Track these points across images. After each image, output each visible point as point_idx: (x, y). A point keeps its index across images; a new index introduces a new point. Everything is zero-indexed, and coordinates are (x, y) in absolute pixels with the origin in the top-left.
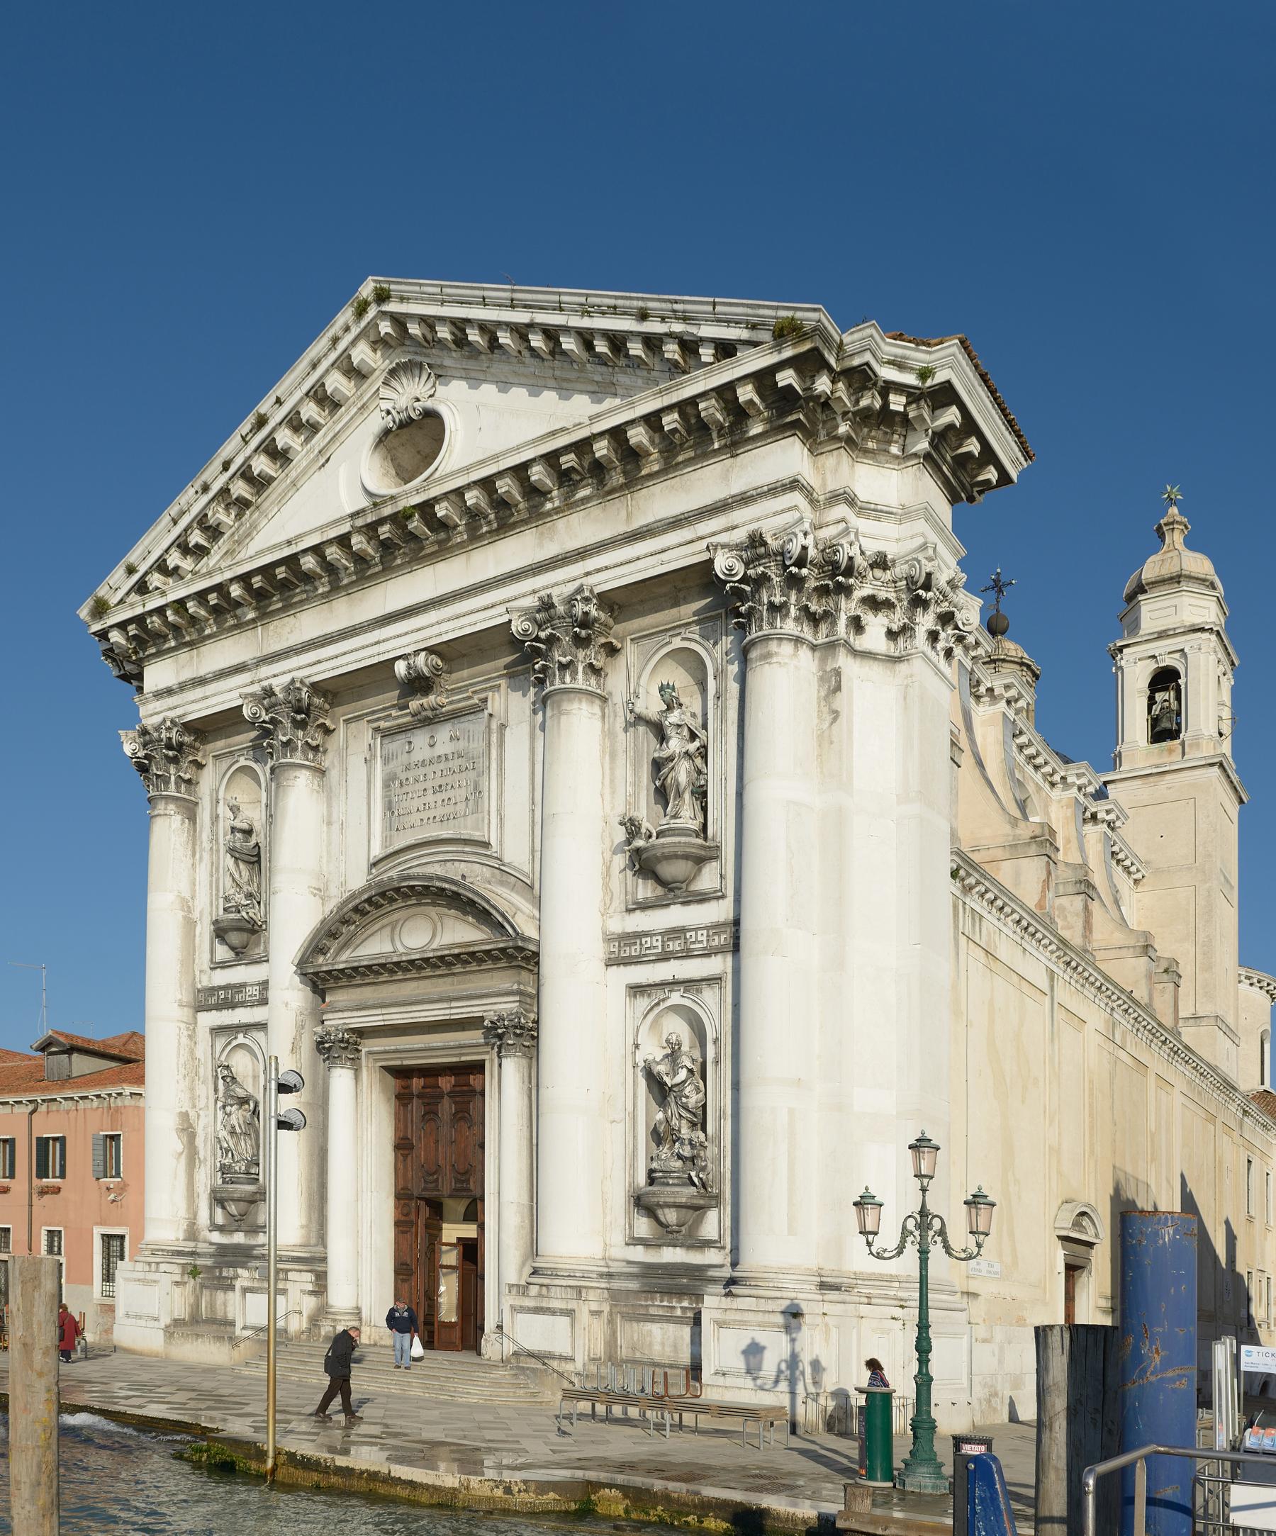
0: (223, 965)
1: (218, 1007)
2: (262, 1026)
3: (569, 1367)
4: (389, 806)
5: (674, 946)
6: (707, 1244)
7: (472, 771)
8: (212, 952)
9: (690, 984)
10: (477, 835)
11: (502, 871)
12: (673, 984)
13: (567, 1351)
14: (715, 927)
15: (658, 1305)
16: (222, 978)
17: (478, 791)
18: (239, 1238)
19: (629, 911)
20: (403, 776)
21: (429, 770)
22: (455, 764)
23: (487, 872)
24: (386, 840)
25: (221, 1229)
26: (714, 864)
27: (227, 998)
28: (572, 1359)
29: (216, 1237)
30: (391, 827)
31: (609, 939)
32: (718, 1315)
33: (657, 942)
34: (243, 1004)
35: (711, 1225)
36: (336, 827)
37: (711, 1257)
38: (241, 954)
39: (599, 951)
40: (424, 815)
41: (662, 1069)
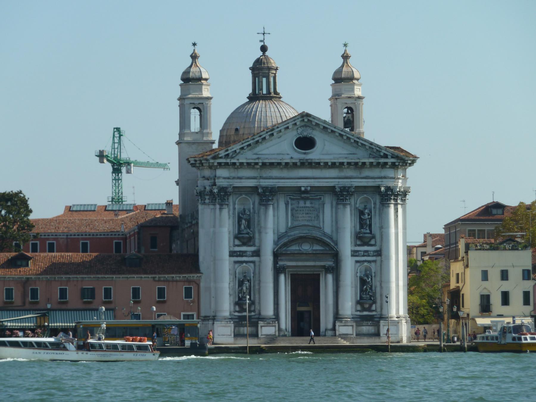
0: (238, 246)
1: (237, 256)
3: (352, 336)
4: (292, 215)
5: (365, 254)
6: (373, 311)
8: (234, 242)
9: (369, 262)
10: (318, 226)
11: (325, 234)
12: (365, 261)
13: (351, 333)
14: (375, 251)
15: (365, 323)
16: (237, 249)
17: (318, 216)
19: (355, 246)
20: (297, 209)
21: (304, 209)
22: (312, 209)
23: (321, 234)
24: (292, 224)
25: (238, 312)
26: (374, 240)
27: (242, 254)
28: (353, 334)
29: (237, 314)
30: (293, 220)
31: (352, 251)
32: (384, 324)
33: (362, 253)
34: (246, 256)
35: (374, 308)
36: (276, 218)
37: (374, 313)
38: (244, 244)
40: (303, 219)
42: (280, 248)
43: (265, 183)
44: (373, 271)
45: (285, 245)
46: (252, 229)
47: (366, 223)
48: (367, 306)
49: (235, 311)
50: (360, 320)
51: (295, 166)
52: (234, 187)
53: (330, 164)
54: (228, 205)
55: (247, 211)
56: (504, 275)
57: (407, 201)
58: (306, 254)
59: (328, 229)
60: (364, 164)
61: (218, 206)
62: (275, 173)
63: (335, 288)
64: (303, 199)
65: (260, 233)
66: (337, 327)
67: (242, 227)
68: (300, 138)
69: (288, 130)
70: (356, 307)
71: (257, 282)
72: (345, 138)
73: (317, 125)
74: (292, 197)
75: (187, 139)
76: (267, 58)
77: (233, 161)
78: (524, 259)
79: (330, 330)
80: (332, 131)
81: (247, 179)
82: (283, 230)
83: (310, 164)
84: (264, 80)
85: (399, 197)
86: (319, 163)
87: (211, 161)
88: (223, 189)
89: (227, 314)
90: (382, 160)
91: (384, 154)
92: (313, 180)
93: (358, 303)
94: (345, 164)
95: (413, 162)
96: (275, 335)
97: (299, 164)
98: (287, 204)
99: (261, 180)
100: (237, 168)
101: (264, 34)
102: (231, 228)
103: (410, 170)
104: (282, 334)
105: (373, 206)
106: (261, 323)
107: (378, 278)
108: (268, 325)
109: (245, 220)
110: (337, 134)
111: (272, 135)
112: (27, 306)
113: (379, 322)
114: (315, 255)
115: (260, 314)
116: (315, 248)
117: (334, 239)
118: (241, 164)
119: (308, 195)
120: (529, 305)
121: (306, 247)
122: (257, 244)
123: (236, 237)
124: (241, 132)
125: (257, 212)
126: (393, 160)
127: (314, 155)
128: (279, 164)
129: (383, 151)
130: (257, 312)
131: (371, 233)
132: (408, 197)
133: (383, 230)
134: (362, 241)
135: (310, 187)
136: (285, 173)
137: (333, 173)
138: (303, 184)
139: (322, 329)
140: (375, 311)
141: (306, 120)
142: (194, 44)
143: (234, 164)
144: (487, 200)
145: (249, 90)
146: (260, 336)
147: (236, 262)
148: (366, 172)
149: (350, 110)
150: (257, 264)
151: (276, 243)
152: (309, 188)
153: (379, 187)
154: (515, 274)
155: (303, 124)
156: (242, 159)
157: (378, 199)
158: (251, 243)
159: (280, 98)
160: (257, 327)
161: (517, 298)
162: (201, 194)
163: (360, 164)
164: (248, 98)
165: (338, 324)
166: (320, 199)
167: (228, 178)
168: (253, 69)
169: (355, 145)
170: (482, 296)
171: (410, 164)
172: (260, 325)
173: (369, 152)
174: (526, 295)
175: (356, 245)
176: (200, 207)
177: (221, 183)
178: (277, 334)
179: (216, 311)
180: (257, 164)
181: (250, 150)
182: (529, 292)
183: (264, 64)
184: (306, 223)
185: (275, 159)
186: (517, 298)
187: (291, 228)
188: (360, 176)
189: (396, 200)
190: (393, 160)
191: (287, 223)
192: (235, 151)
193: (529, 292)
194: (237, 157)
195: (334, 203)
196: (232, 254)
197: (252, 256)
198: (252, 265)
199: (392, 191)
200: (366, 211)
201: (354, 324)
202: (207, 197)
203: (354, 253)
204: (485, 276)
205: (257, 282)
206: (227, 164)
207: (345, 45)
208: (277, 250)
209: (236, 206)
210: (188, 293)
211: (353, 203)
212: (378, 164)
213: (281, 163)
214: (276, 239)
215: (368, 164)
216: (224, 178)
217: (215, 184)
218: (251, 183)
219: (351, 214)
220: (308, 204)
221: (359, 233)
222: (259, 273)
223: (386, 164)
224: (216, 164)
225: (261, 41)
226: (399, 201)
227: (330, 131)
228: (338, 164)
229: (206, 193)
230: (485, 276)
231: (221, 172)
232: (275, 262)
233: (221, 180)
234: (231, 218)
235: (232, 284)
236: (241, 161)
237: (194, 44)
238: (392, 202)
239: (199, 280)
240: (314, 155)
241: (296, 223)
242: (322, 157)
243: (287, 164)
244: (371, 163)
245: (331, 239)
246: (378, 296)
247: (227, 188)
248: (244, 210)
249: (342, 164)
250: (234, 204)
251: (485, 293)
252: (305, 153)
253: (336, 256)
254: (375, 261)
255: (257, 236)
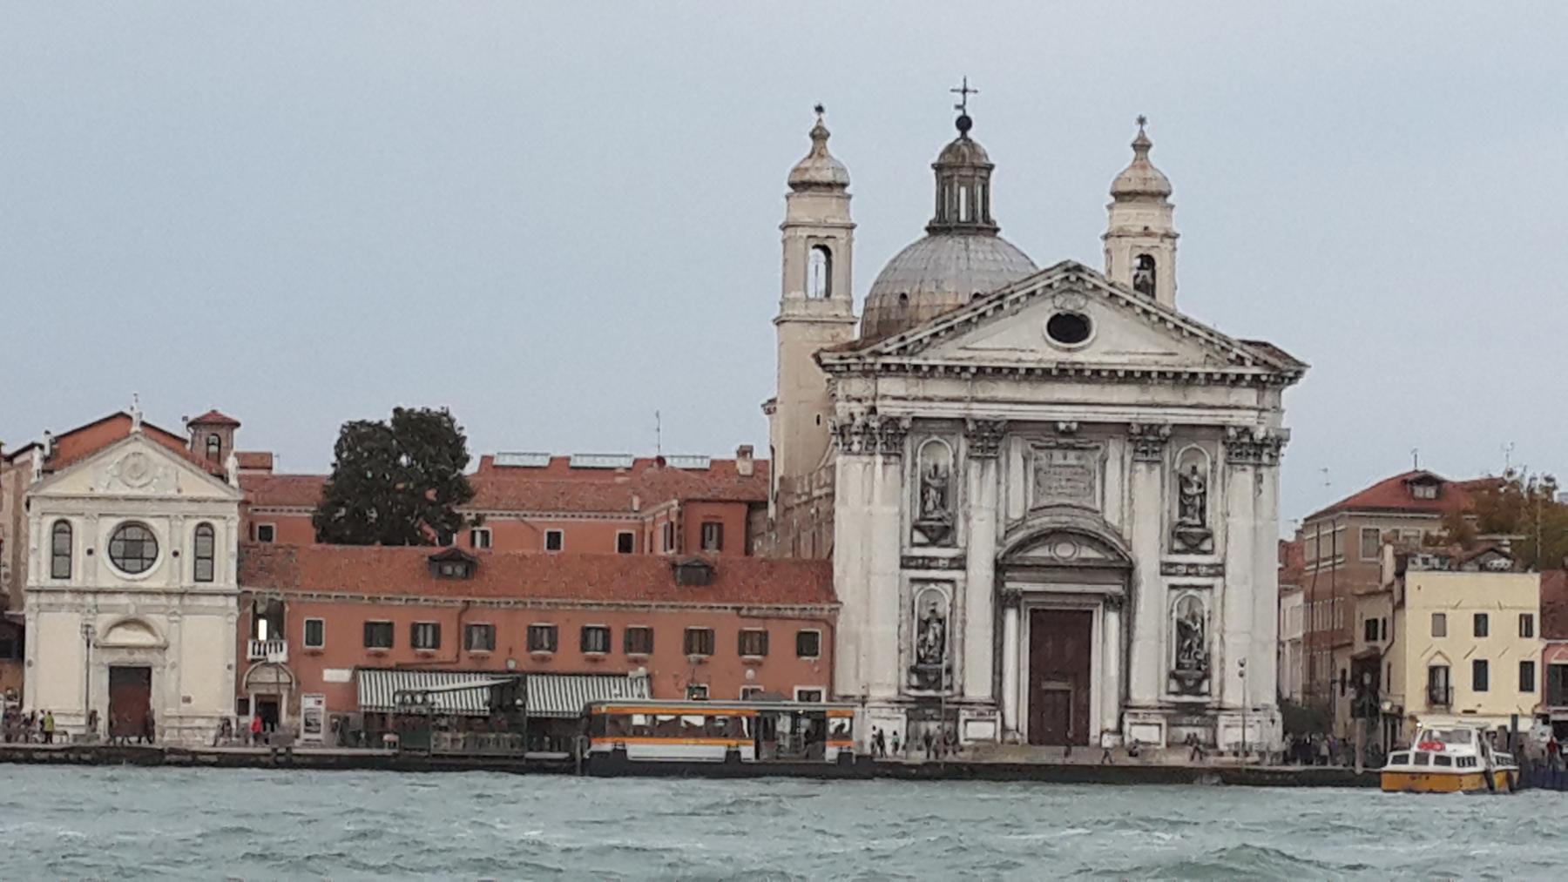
1: (917, 568)
2: (951, 581)
4: (1038, 483)
7: (1092, 478)
13: (1155, 738)
15: (1185, 720)
16: (917, 552)
17: (1092, 488)
18: (931, 693)
24: (1036, 500)
25: (917, 688)
27: (927, 563)
29: (913, 692)
31: (1163, 564)
34: (936, 568)
35: (1205, 687)
36: (1003, 488)
37: (1205, 699)
38: (933, 542)
39: (1156, 568)
41: (1189, 622)
42: (1012, 551)
43: (980, 411)
44: (1206, 608)
45: (1022, 546)
46: (950, 510)
47: (1192, 505)
48: (1191, 683)
49: (910, 687)
50: (1176, 713)
51: (1048, 375)
52: (914, 419)
53: (1121, 374)
54: (899, 456)
55: (941, 470)
56: (1481, 625)
57: (1281, 460)
58: (1063, 567)
59: (1112, 517)
60: (1194, 375)
61: (879, 459)
62: (1003, 390)
63: (1124, 642)
64: (1059, 446)
65: (967, 519)
66: (1126, 728)
67: (930, 505)
68: (1058, 315)
69: (1034, 299)
70: (1168, 685)
71: (958, 625)
72: (1155, 318)
73: (1096, 288)
74: (1038, 443)
75: (799, 311)
76: (968, 142)
77: (915, 361)
78: (1522, 591)
79: (1114, 733)
80: (1128, 303)
81: (943, 400)
82: (1016, 514)
83: (1079, 372)
84: (963, 191)
85: (1266, 450)
86: (1097, 372)
87: (870, 360)
88: (894, 421)
89: (892, 693)
90: (1233, 370)
91: (1238, 356)
92: (1082, 409)
93: (1172, 675)
94: (1154, 375)
95: (1298, 374)
96: (994, 740)
97: (1055, 372)
98: (1025, 460)
99: (975, 405)
100: (924, 377)
101: (965, 91)
102: (907, 509)
103: (1288, 392)
104: (1009, 737)
105: (1209, 467)
106: (964, 714)
107: (1217, 623)
108: (981, 717)
109: (936, 489)
110: (1138, 310)
111: (1001, 307)
112: (465, 663)
113: (1215, 718)
114: (1083, 569)
115: (962, 694)
116: (1083, 555)
117: (1126, 537)
118: (933, 368)
119: (1071, 441)
120: (1532, 690)
121: (1065, 552)
122: (961, 544)
123: (916, 527)
124: (912, 302)
125: (962, 473)
126: (1256, 370)
127: (1088, 354)
128: (1013, 371)
129: (1236, 351)
130: (957, 689)
131: (1203, 525)
132: (1283, 450)
133: (1229, 520)
134: (1184, 542)
135: (1080, 423)
136: (1025, 391)
137: (1129, 393)
138: (1064, 415)
139: (1094, 731)
140: (1209, 694)
141: (1073, 278)
142: (819, 109)
143: (917, 368)
144: (1406, 468)
145: (932, 215)
146: (962, 741)
147: (913, 580)
148: (1199, 395)
149: (1147, 261)
150: (960, 585)
151: (999, 542)
152: (1074, 426)
153: (1222, 427)
154: (1503, 625)
155: (1066, 285)
156: (934, 357)
157: (1221, 451)
158: (948, 541)
159: (996, 230)
160: (957, 722)
161: (1504, 676)
162: (842, 431)
163: (1186, 376)
164: (928, 229)
165: (1127, 720)
166: (1098, 448)
167: (904, 399)
168: (938, 168)
169: (1176, 335)
170: (1433, 671)
171: (1291, 379)
172: (962, 719)
173: (1205, 352)
174: (1526, 668)
175: (1172, 551)
176: (840, 460)
177: (888, 409)
178: (999, 738)
179: (867, 687)
180: (965, 369)
181: (952, 339)
182: (1532, 663)
183: (964, 156)
184: (1067, 501)
185: (1004, 360)
186: (1504, 676)
187: (1033, 510)
188: (1183, 402)
189: (1258, 456)
190: (1256, 370)
191: (1026, 498)
192: (921, 341)
193: (1532, 663)
194: (922, 355)
195: (1128, 459)
196: (906, 563)
197: (950, 568)
198: (948, 587)
199: (1251, 438)
200: (1196, 478)
201: (1164, 722)
202: (856, 439)
203: (1167, 569)
204: (1439, 625)
205: (958, 625)
206: (902, 367)
207: (1142, 121)
208: (1004, 558)
209: (919, 460)
210: (806, 644)
211: (1167, 460)
212: (1224, 376)
213: (1017, 369)
214: (1002, 533)
215: (1201, 376)
216: (895, 398)
217: (873, 410)
218: (953, 410)
219: (1163, 486)
220: (1072, 455)
221: (1181, 524)
222: (964, 608)
223: (1240, 377)
224: (878, 367)
225: (958, 107)
226: (1265, 459)
227: (1122, 302)
228: (1137, 375)
229: (854, 429)
230: (1439, 625)
231: (888, 385)
232: (998, 582)
233: (888, 402)
234: (908, 485)
235: (904, 628)
236: (931, 362)
237: (819, 109)
238: (1251, 460)
239: (835, 617)
240: (1088, 354)
241: (1044, 502)
242: (1106, 359)
243: (1030, 371)
244: (1209, 375)
245: (1120, 536)
246: (1215, 662)
247: (899, 419)
248: (936, 467)
249: (1146, 375)
250: (914, 456)
251: (1439, 661)
252: (1069, 350)
253: (1127, 571)
254: (1210, 587)
255: (961, 525)
